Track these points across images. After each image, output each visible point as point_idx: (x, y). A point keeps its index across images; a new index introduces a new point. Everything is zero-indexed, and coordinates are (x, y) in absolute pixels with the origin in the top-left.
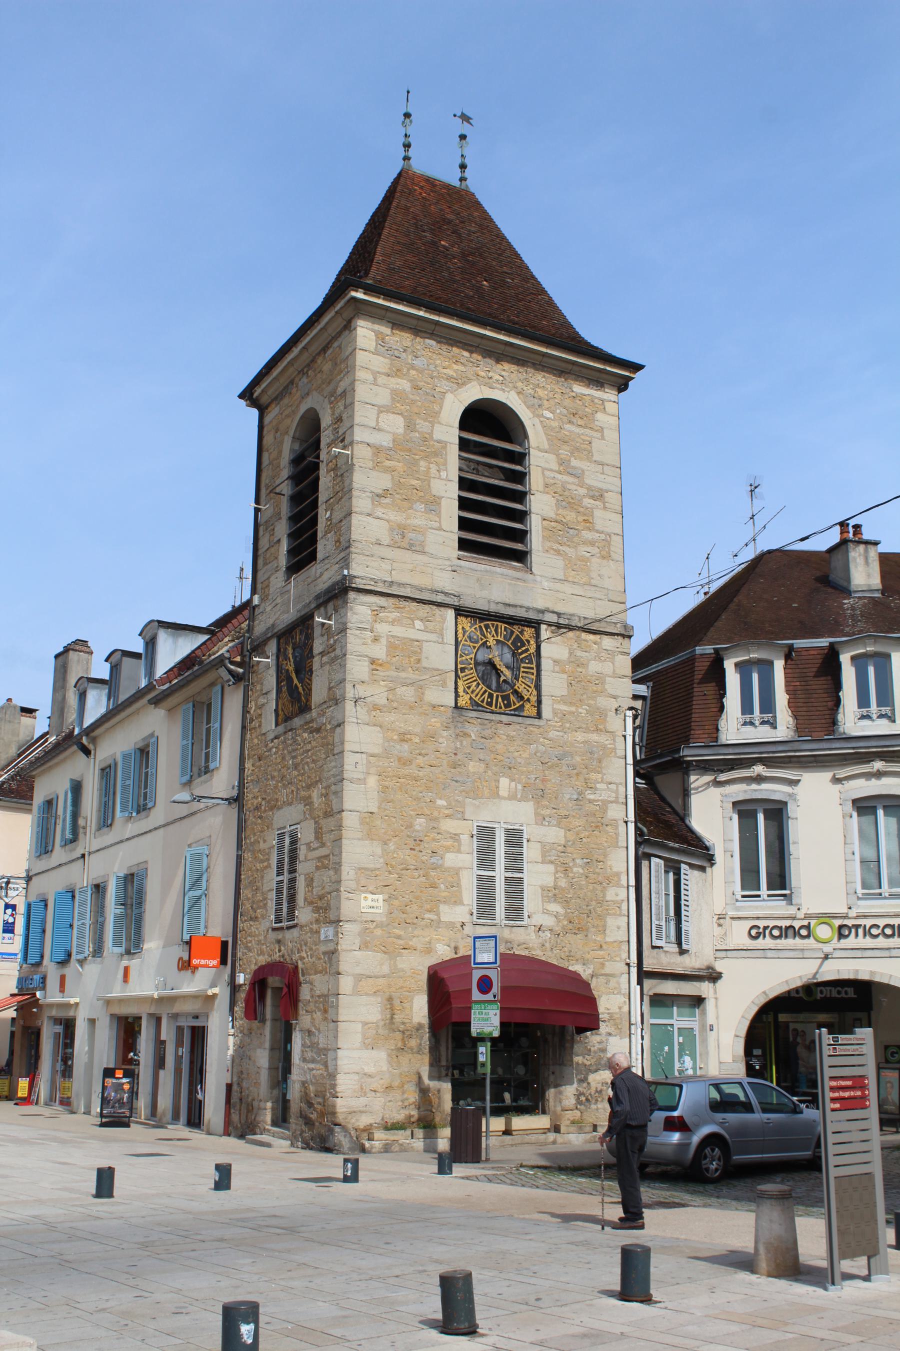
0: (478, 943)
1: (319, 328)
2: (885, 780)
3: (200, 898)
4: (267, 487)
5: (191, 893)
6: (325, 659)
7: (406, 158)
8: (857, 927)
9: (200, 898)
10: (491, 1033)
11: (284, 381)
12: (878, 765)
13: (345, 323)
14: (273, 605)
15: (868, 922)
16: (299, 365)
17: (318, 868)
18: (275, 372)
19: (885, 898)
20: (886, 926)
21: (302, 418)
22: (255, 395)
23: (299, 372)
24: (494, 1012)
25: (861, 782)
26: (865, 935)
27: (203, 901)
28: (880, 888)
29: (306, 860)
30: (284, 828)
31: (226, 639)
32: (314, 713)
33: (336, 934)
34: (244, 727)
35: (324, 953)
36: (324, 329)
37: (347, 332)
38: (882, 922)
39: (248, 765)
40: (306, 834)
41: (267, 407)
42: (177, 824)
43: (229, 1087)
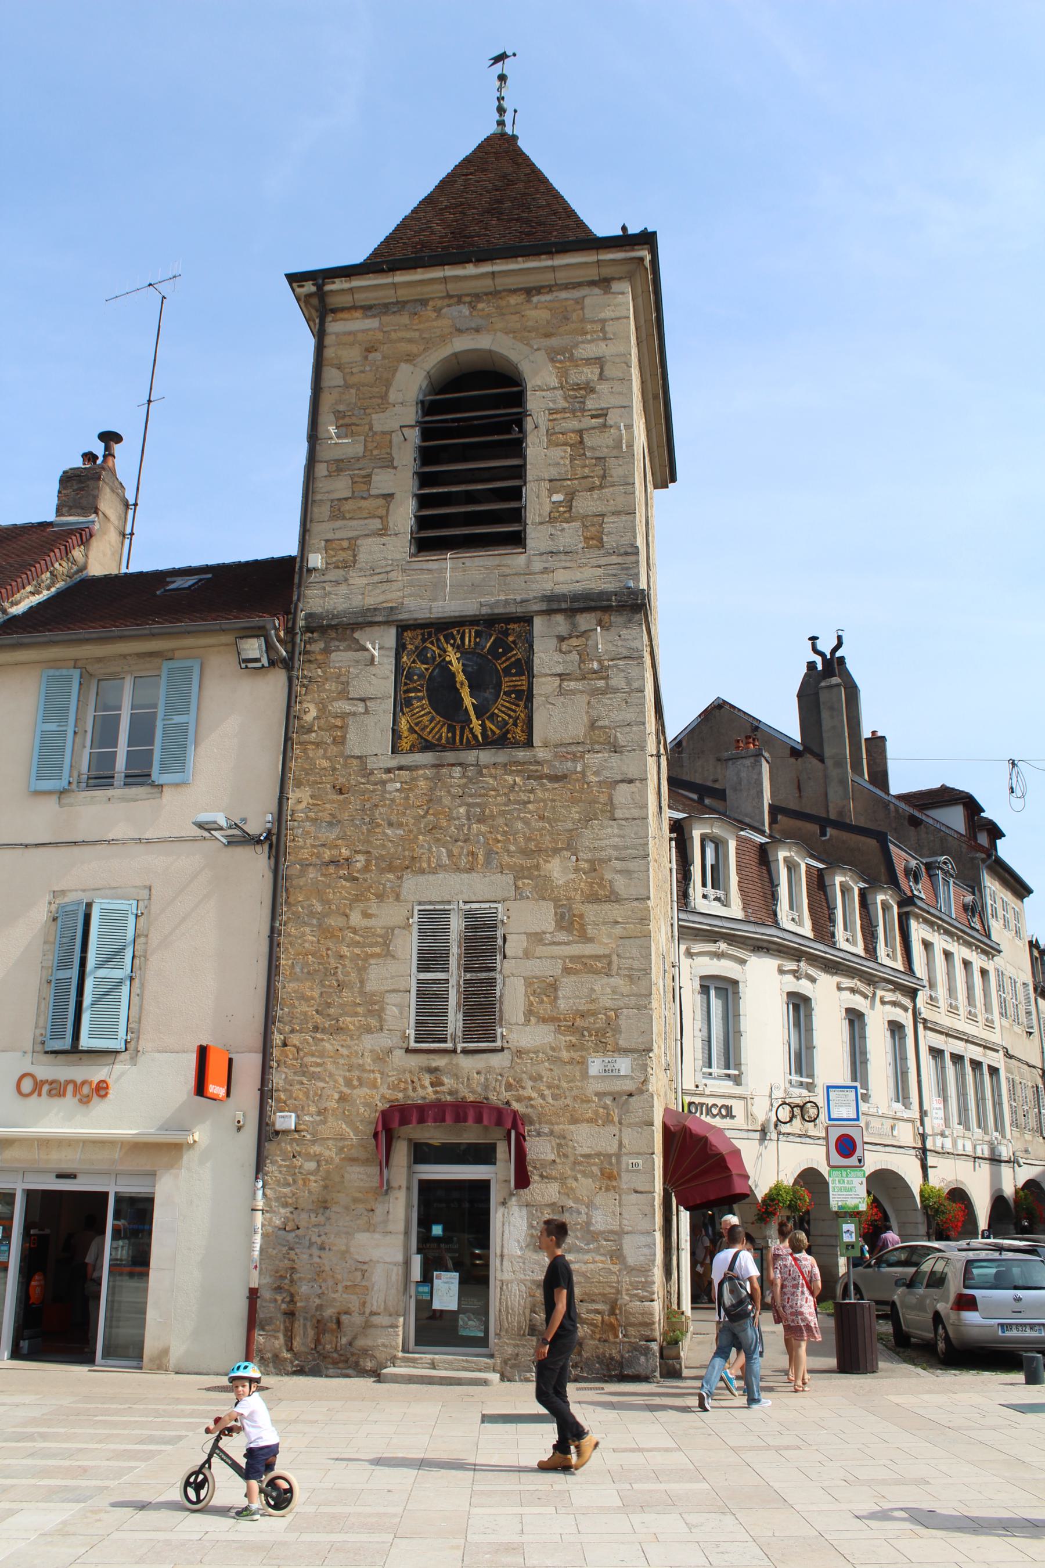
0: (833, 1094)
1: (549, 263)
2: (724, 962)
3: (120, 983)
4: (339, 415)
5: (118, 974)
6: (573, 685)
7: (501, 123)
8: (702, 1104)
9: (120, 983)
10: (857, 1207)
11: (403, 294)
12: (723, 946)
13: (597, 278)
14: (376, 578)
15: (710, 1101)
16: (453, 288)
17: (567, 971)
18: (400, 277)
19: (715, 1078)
20: (723, 1106)
21: (455, 355)
22: (328, 288)
23: (449, 296)
24: (860, 1180)
25: (706, 959)
26: (707, 1114)
27: (125, 989)
28: (710, 1067)
29: (527, 955)
30: (449, 903)
31: (29, 588)
32: (541, 753)
33: (644, 1067)
34: (287, 739)
35: (597, 1094)
36: (553, 268)
37: (596, 291)
38: (720, 1102)
39: (293, 795)
40: (523, 921)
41: (334, 311)
42: (19, 852)
43: (253, 1294)
